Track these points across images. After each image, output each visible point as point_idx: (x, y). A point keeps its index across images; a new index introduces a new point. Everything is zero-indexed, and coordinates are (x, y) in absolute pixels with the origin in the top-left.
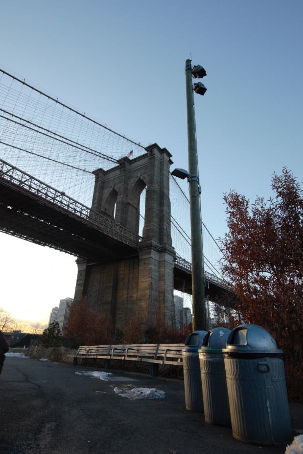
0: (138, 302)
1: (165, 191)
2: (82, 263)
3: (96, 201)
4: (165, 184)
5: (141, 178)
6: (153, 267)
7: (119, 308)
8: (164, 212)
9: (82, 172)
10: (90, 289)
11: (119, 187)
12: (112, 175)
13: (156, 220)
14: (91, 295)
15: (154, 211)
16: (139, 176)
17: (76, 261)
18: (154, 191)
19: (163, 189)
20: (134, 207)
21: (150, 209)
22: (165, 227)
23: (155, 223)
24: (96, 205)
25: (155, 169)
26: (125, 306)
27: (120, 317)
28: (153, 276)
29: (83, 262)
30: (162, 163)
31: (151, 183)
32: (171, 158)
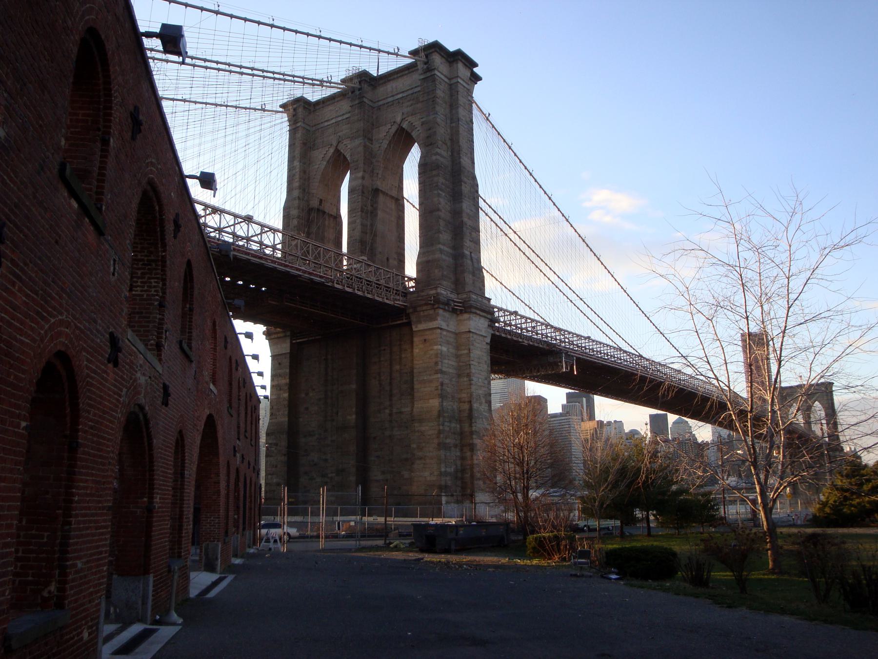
0: (416, 425)
1: (465, 161)
2: (278, 338)
3: (296, 184)
4: (463, 143)
5: (405, 125)
6: (444, 349)
7: (375, 438)
8: (464, 215)
9: (259, 114)
10: (303, 395)
11: (351, 148)
12: (328, 112)
13: (445, 237)
14: (307, 409)
15: (439, 217)
16: (399, 119)
17: (264, 333)
18: (437, 167)
19: (460, 158)
20: (392, 197)
21: (431, 212)
22: (467, 252)
23: (444, 245)
24: (296, 193)
25: (438, 108)
26: (387, 433)
27: (378, 457)
28: (444, 369)
29: (281, 335)
30: (453, 89)
31: (431, 144)
32: (475, 70)
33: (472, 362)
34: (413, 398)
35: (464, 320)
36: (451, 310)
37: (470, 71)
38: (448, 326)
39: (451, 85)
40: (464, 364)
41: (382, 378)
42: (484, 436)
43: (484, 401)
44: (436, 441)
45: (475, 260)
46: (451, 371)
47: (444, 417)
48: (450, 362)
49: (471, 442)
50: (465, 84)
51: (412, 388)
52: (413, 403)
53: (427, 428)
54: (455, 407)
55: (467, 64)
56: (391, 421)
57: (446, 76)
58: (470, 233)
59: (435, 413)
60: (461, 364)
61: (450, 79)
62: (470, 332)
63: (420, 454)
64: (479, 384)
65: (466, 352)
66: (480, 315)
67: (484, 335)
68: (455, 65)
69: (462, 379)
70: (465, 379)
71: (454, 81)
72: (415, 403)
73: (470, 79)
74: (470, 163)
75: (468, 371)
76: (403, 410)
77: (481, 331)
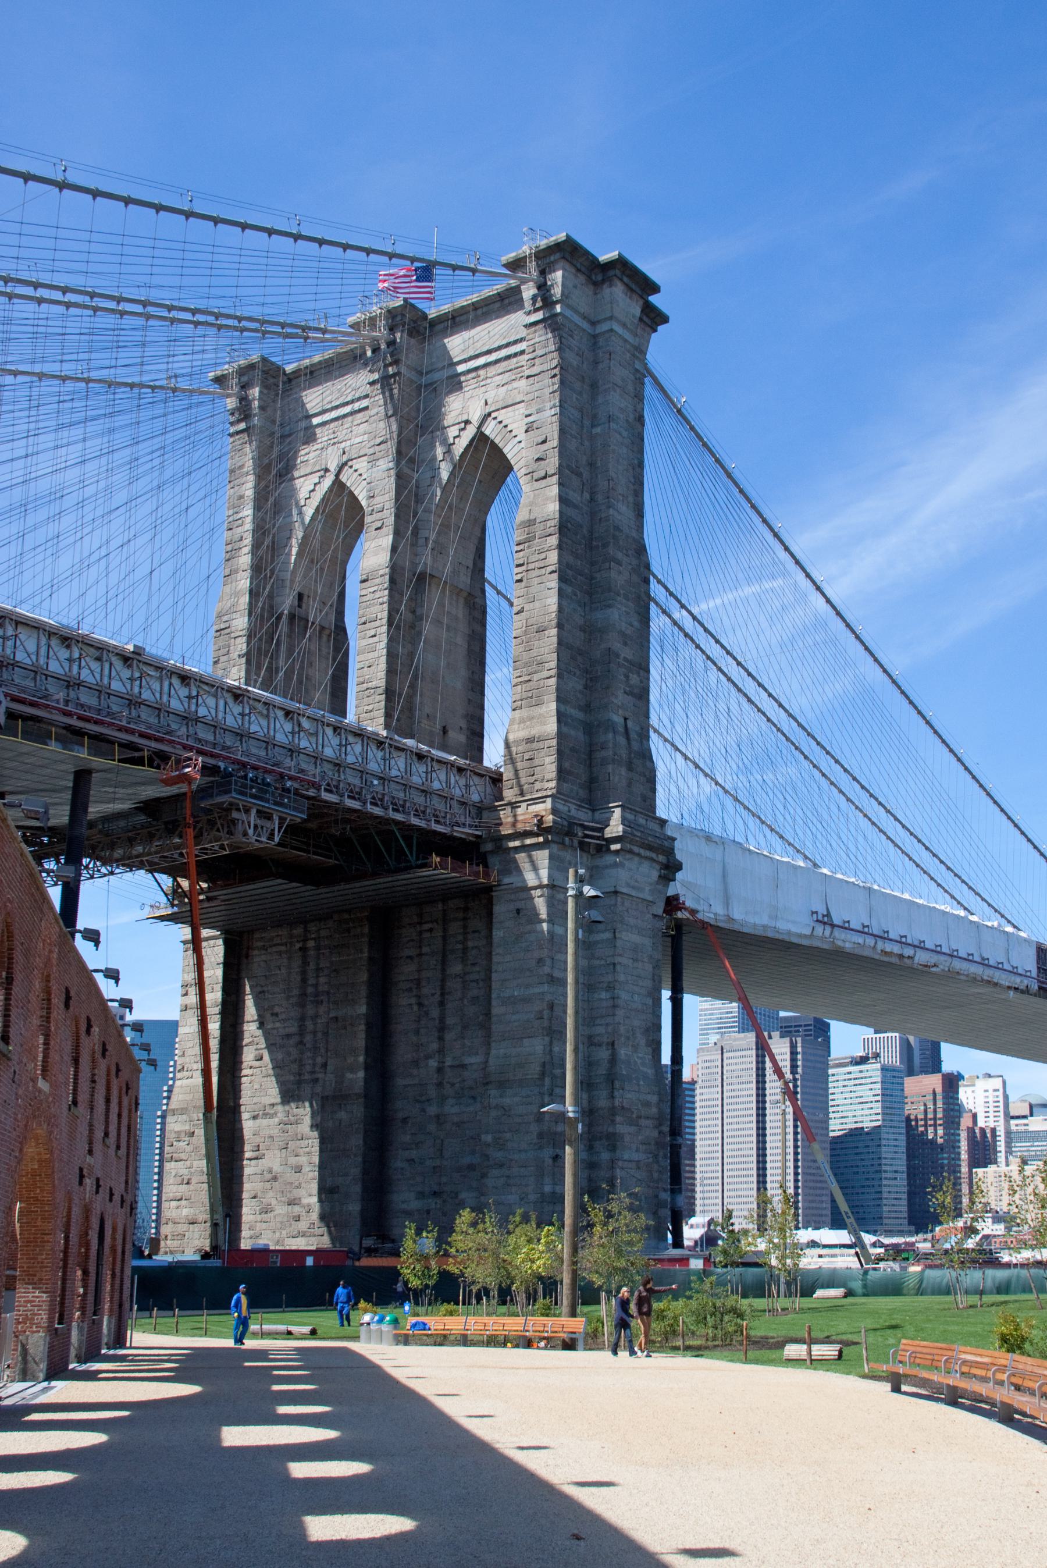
1: (621, 513)
32: (653, 299)
33: (618, 959)
34: (489, 1037)
35: (607, 867)
36: (576, 843)
39: (595, 337)
40: (603, 962)
41: (425, 991)
42: (639, 1117)
43: (643, 1042)
44: (534, 1128)
45: (633, 735)
49: (611, 1130)
50: (627, 336)
51: (488, 1014)
52: (488, 1044)
53: (517, 1099)
55: (633, 286)
56: (440, 1085)
57: (584, 317)
58: (627, 677)
59: (535, 1069)
60: (597, 962)
61: (593, 324)
62: (616, 892)
63: (499, 1155)
65: (607, 935)
66: (638, 855)
67: (650, 898)
68: (606, 291)
69: (596, 996)
70: (603, 995)
71: (604, 327)
72: (493, 1044)
75: (610, 978)
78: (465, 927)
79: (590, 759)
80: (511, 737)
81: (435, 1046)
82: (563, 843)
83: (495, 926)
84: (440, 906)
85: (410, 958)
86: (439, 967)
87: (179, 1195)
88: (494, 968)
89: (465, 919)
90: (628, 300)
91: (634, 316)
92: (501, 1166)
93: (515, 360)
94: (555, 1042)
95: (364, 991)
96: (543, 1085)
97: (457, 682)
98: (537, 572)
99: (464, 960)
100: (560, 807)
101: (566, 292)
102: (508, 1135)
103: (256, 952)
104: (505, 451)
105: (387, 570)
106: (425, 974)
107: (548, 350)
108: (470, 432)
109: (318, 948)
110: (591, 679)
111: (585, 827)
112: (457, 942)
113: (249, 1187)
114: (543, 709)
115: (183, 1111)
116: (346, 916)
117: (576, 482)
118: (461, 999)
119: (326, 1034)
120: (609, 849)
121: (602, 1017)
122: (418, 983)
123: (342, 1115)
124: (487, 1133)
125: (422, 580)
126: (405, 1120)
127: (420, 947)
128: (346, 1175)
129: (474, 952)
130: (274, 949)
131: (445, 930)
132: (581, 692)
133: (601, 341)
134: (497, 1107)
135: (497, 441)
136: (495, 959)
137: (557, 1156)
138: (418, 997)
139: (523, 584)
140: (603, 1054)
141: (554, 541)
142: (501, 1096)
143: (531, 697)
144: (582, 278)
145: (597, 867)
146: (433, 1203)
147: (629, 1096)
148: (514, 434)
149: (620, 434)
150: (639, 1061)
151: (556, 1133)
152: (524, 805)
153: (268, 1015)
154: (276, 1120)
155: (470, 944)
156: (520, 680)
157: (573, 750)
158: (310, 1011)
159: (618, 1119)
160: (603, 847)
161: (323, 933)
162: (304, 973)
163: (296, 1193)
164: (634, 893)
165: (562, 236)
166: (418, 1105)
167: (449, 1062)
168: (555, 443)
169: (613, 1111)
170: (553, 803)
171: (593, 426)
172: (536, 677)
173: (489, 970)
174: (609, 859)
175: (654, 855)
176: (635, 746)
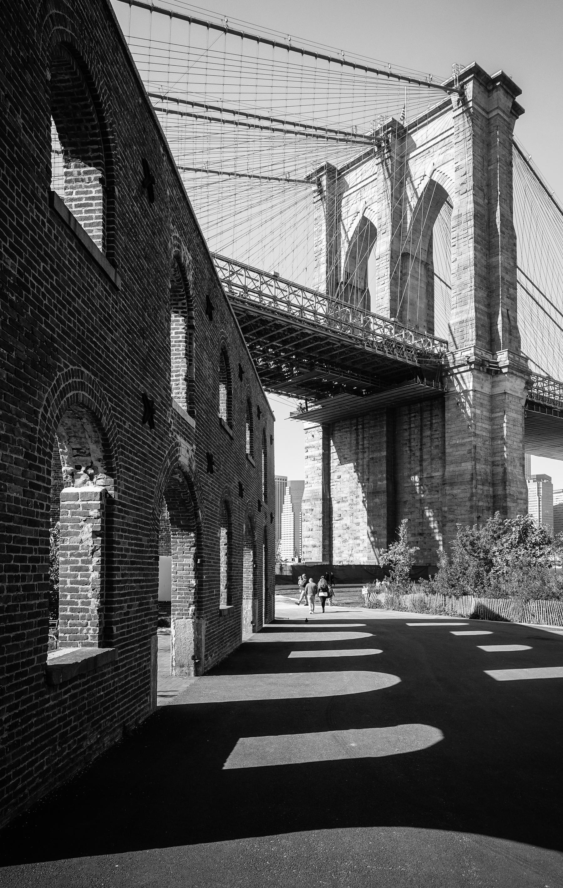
28: (477, 432)
34: (445, 463)
35: (500, 381)
36: (485, 370)
37: (512, 100)
38: (482, 388)
41: (413, 444)
44: (468, 504)
45: (511, 318)
46: (484, 434)
47: (477, 480)
48: (484, 425)
49: (504, 505)
51: (444, 453)
52: (444, 467)
53: (459, 491)
54: (488, 470)
55: (509, 91)
58: (508, 290)
59: (468, 477)
60: (495, 427)
62: (505, 393)
63: (451, 517)
64: (514, 447)
66: (516, 375)
67: (521, 396)
68: (495, 94)
69: (495, 442)
72: (447, 467)
73: (511, 112)
74: (509, 210)
76: (434, 474)
77: (517, 392)
78: (431, 414)
79: (491, 330)
80: (451, 322)
81: (418, 468)
82: (479, 370)
83: (446, 412)
84: (419, 405)
85: (406, 429)
86: (419, 433)
87: (308, 535)
88: (446, 431)
89: (431, 410)
90: (506, 99)
91: (508, 107)
92: (452, 521)
93: (447, 139)
94: (477, 464)
95: (385, 445)
96: (472, 484)
97: (421, 304)
98: (463, 240)
99: (431, 429)
100: (477, 352)
101: (475, 96)
102: (455, 507)
103: (336, 432)
104: (444, 186)
105: (389, 252)
106: (412, 437)
107: (466, 127)
108: (427, 180)
109: (363, 428)
110: (490, 292)
111: (489, 362)
112: (428, 421)
113: (335, 533)
114: (467, 307)
115: (308, 500)
116: (375, 413)
117: (481, 194)
118: (430, 447)
119: (368, 466)
120: (501, 372)
121: (499, 452)
122: (409, 440)
123: (377, 500)
124: (445, 506)
125: (405, 255)
126: (405, 502)
127: (410, 425)
128: (380, 526)
129: (435, 425)
130: (344, 430)
131: (421, 416)
132: (485, 298)
133: (492, 121)
134: (449, 495)
135: (439, 182)
136: (446, 427)
137: (479, 517)
138: (410, 447)
139: (456, 247)
140: (500, 470)
141: (472, 223)
142: (451, 489)
143: (461, 302)
144: (482, 88)
145: (495, 381)
146: (419, 539)
147: (513, 489)
148: (448, 177)
149: (503, 168)
150: (517, 473)
151: (478, 506)
152: (460, 352)
153: (342, 459)
154: (348, 503)
155: (434, 421)
156: (455, 294)
157: (482, 325)
158: (360, 456)
159: (508, 499)
160: (498, 372)
161: (365, 421)
162: (357, 440)
163: (358, 534)
164: (513, 394)
165: (473, 64)
166: (411, 495)
167: (425, 475)
168: (471, 174)
169: (505, 496)
170: (475, 350)
171: (489, 166)
172: (463, 292)
173: (444, 433)
174: (501, 377)
175: (523, 375)
176: (513, 323)
